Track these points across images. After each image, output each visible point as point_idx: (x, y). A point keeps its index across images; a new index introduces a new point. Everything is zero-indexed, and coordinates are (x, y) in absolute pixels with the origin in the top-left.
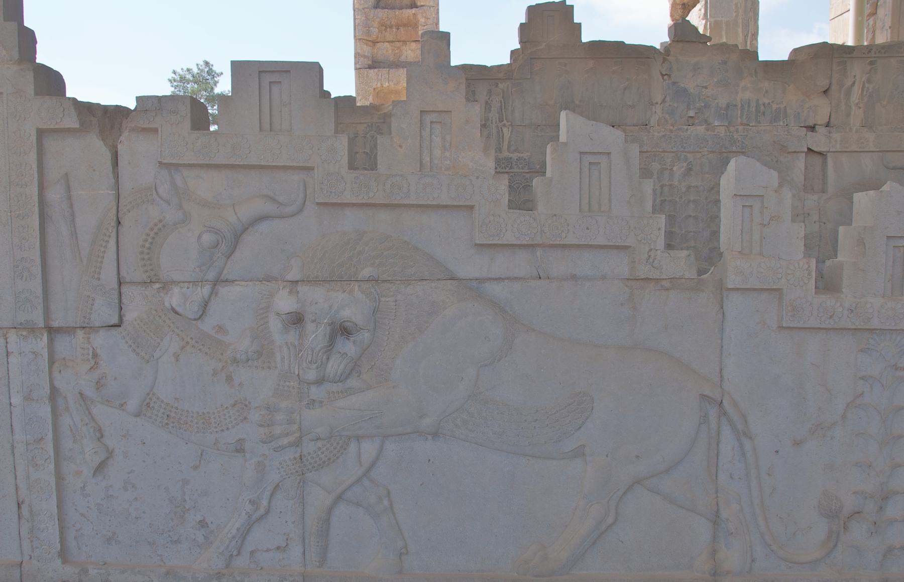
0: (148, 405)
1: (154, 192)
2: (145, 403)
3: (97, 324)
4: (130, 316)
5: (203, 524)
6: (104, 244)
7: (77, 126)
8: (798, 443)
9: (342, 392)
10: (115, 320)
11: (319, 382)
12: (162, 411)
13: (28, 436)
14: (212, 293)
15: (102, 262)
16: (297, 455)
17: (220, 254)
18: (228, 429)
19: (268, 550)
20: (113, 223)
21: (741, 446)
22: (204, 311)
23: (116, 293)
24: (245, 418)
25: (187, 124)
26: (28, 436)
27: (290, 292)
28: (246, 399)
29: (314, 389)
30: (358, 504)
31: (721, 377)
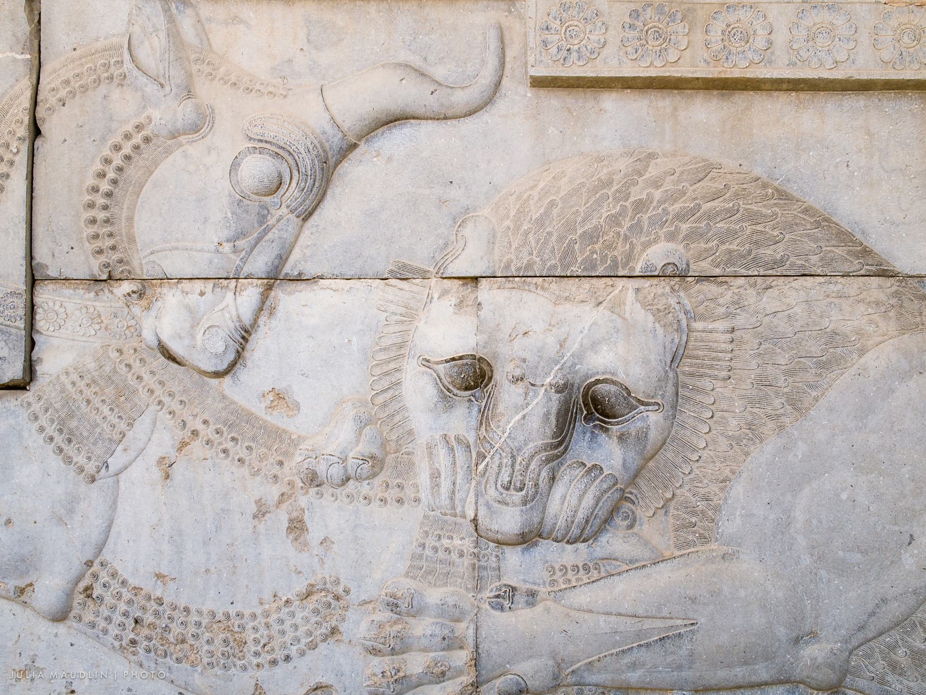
0: (88, 589)
1: (127, 56)
2: (82, 585)
4: (53, 361)
9: (586, 568)
10: (14, 371)
11: (527, 539)
12: (122, 607)
14: (261, 309)
17: (284, 210)
18: (288, 658)
20: (23, 131)
22: (239, 355)
23: (20, 304)
24: (334, 631)
27: (460, 305)
28: (337, 582)
29: (513, 557)
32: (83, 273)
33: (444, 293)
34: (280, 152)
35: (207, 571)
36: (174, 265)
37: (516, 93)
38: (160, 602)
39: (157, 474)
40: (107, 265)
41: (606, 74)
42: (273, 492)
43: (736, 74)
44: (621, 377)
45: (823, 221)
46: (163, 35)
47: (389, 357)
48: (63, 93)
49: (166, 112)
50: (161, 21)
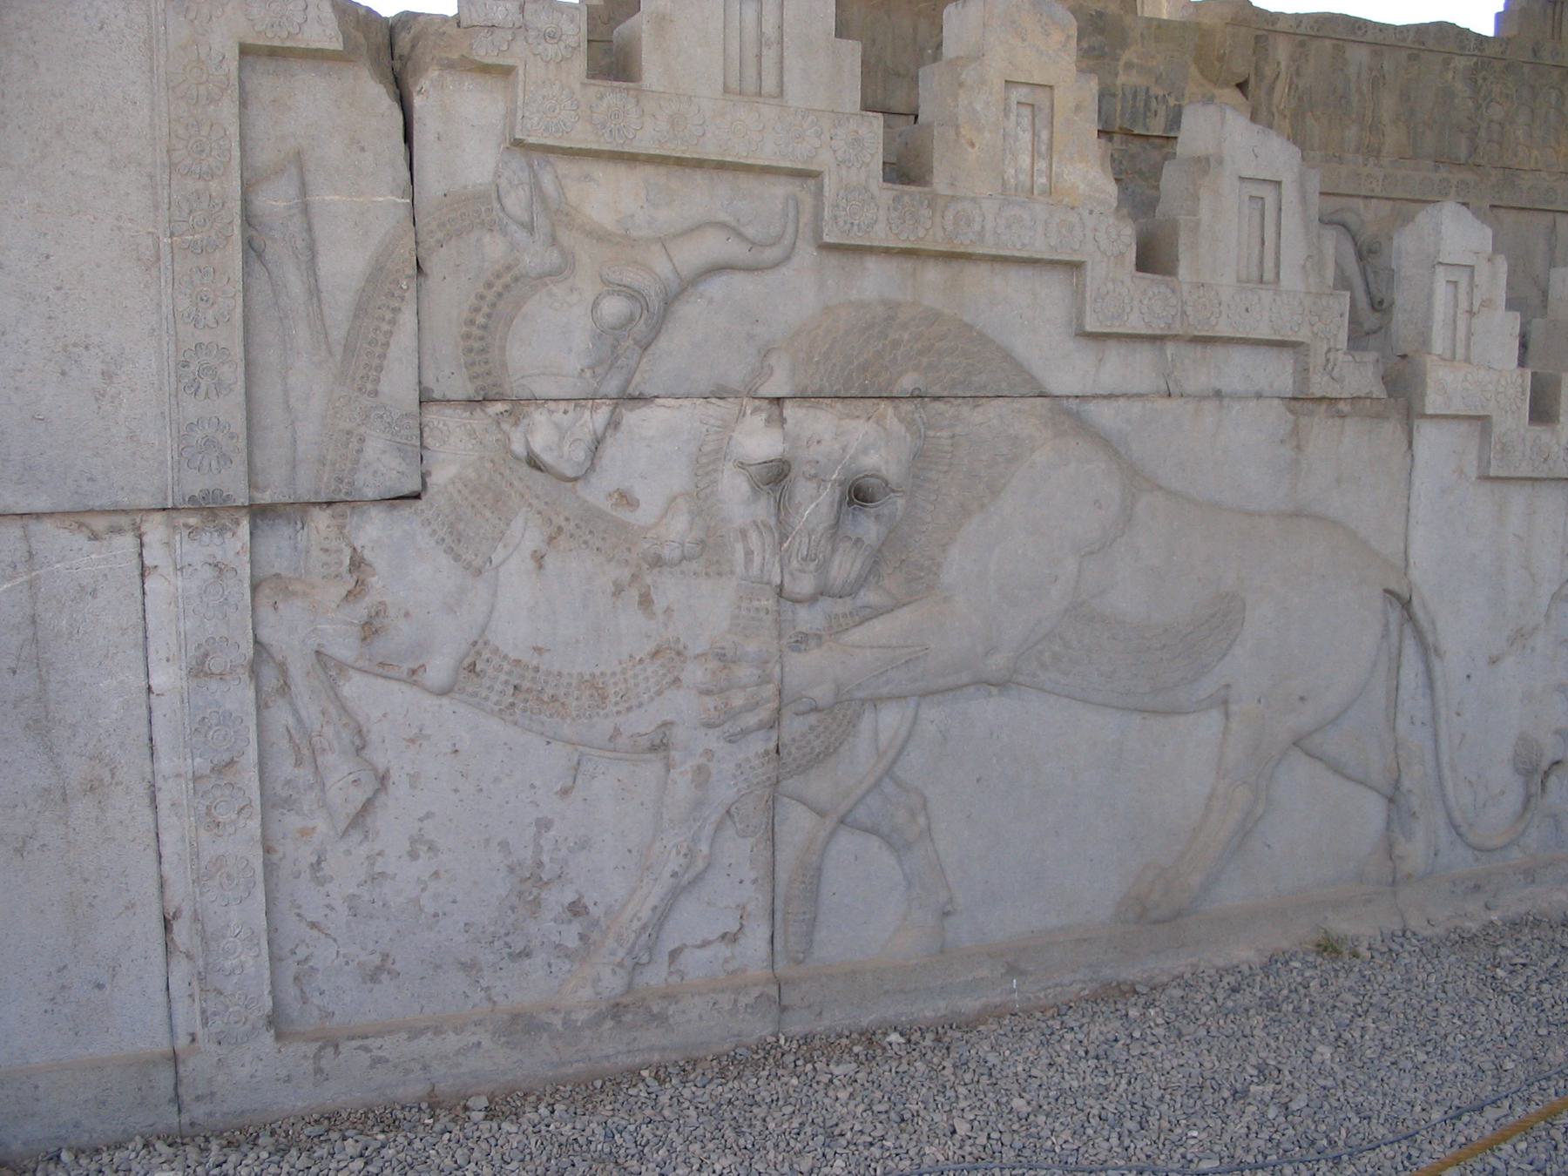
0: (472, 668)
1: (496, 205)
3: (370, 493)
5: (576, 909)
6: (388, 316)
7: (338, 45)
8: (1494, 661)
10: (413, 485)
11: (813, 599)
12: (503, 677)
13: (198, 760)
15: (383, 356)
16: (772, 745)
17: (630, 342)
18: (640, 705)
19: (705, 944)
20: (412, 271)
21: (1429, 671)
24: (677, 680)
25: (580, 65)
26: (198, 760)
27: (768, 421)
30: (872, 831)
31: (1407, 560)
32: (461, 395)
33: (755, 410)
34: (633, 294)
35: (577, 641)
36: (543, 388)
37: (807, 253)
38: (537, 670)
39: (531, 565)
40: (483, 389)
41: (876, 243)
42: (626, 574)
43: (962, 249)
44: (884, 472)
45: (1008, 356)
46: (527, 188)
47: (707, 462)
48: (440, 235)
49: (536, 256)
50: (525, 175)
